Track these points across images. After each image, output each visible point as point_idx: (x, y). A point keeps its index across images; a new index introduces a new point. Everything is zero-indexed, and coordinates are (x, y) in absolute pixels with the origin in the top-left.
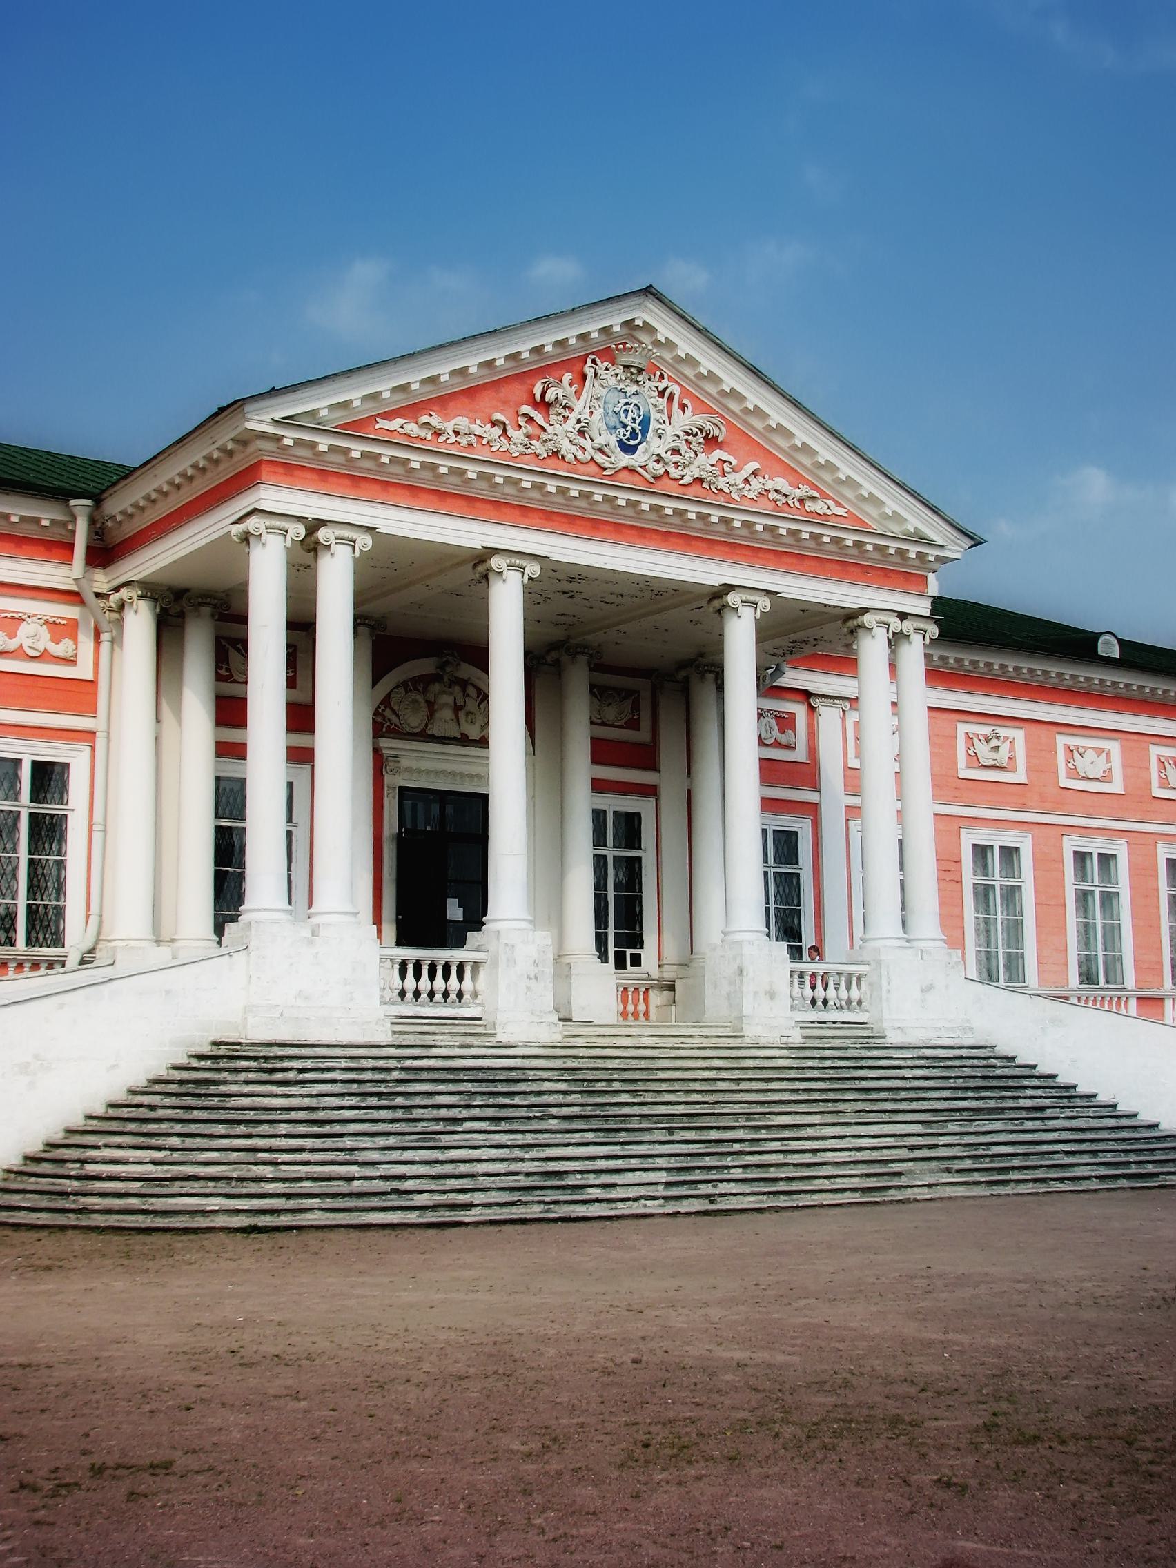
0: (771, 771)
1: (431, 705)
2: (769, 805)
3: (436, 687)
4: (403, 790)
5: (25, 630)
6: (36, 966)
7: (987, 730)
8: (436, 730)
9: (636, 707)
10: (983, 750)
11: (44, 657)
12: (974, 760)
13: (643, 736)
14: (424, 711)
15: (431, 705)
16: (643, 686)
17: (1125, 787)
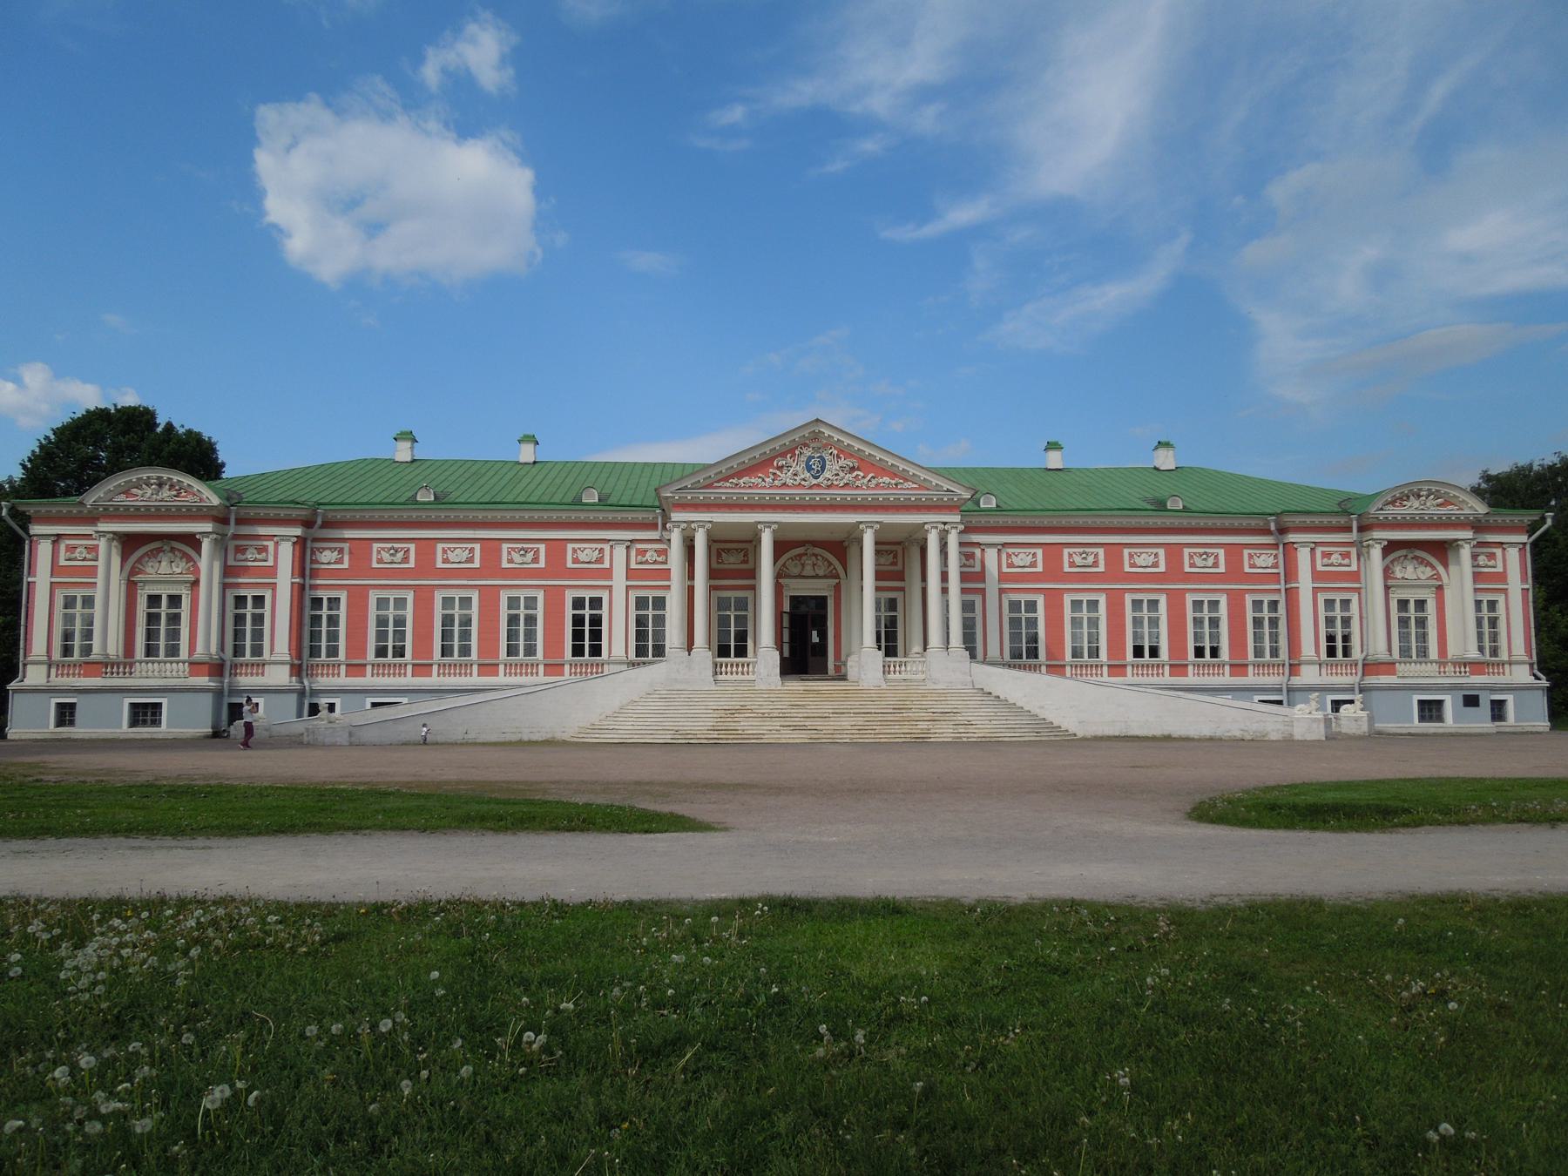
0: (964, 577)
1: (803, 565)
2: (964, 591)
3: (804, 558)
4: (791, 597)
5: (648, 554)
6: (639, 664)
7: (1081, 550)
8: (804, 574)
9: (895, 557)
10: (1078, 560)
11: (655, 562)
12: (1072, 564)
13: (899, 567)
14: (800, 567)
15: (803, 565)
16: (899, 549)
17: (1166, 568)
